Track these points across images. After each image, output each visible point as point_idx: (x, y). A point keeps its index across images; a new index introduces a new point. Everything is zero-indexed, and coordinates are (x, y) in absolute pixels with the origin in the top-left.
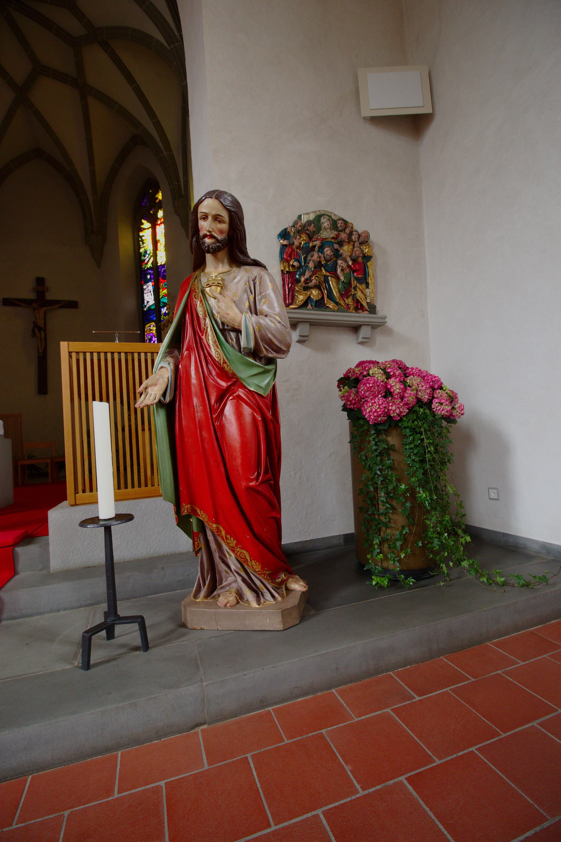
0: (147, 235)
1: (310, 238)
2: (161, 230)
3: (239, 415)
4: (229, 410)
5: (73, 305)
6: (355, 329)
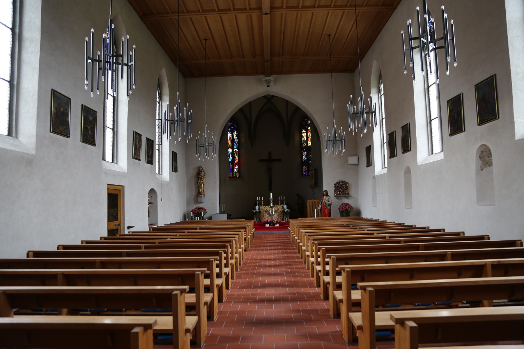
0: (304, 135)
1: (339, 184)
2: (309, 134)
3: (327, 210)
4: (326, 210)
5: (279, 160)
6: (345, 197)
